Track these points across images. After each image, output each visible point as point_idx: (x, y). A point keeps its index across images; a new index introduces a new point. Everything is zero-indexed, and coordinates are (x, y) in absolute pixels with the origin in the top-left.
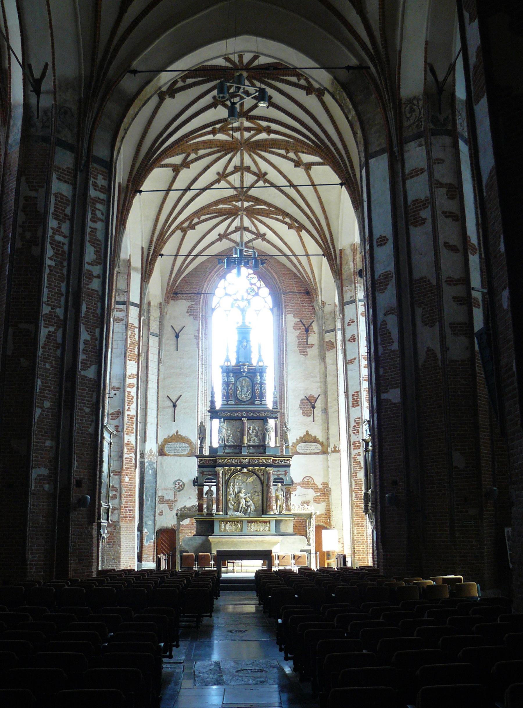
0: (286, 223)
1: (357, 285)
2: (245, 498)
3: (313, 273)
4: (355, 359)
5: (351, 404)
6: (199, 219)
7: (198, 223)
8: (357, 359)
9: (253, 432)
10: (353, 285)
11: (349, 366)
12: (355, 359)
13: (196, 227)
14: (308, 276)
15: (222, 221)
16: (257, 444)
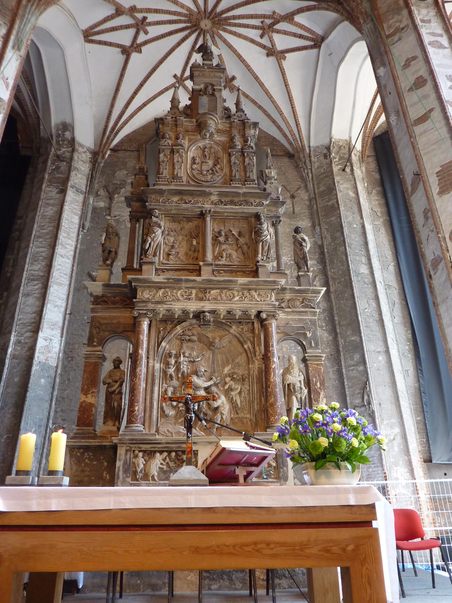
0: (264, 47)
1: (413, 8)
2: (207, 389)
3: (297, 125)
4: (431, 110)
5: (435, 189)
6: (146, 33)
7: (146, 43)
8: (438, 110)
9: (227, 239)
10: (405, 12)
11: (418, 129)
12: (431, 110)
13: (143, 48)
14: (291, 131)
15: (179, 44)
16: (236, 263)
